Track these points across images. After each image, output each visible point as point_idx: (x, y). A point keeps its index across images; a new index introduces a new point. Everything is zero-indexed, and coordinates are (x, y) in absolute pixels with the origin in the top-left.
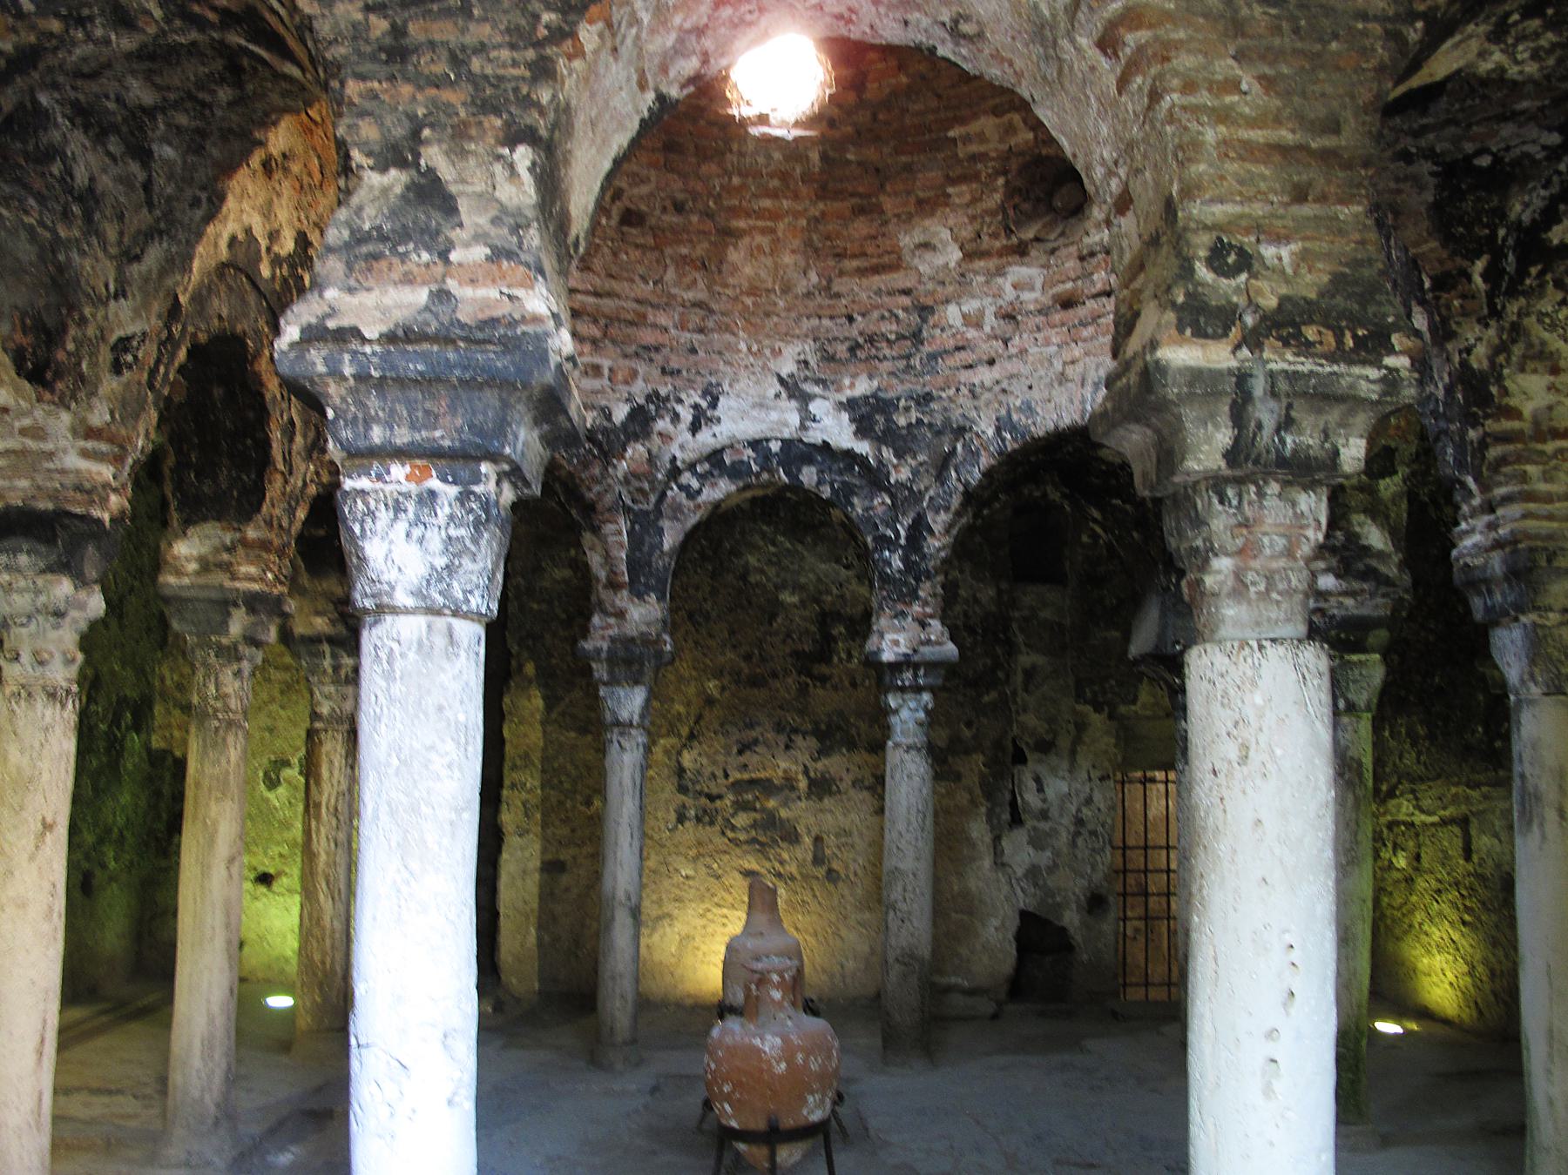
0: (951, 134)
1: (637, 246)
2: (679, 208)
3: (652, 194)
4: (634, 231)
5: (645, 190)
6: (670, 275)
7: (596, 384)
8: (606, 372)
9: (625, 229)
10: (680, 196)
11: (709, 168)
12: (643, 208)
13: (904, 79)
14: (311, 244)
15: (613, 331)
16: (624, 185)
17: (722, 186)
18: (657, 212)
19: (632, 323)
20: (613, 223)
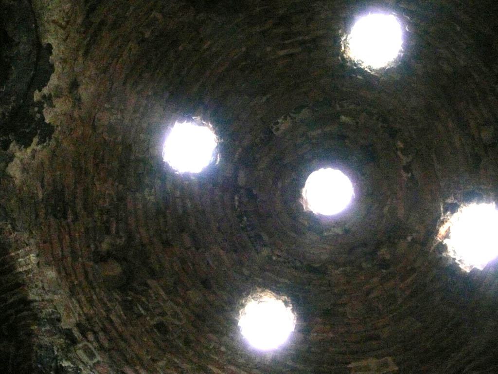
0: (350, 366)
1: (155, 342)
2: (187, 342)
3: (178, 326)
4: (159, 335)
5: (177, 323)
6: (161, 364)
7: (85, 358)
8: (95, 361)
9: (155, 330)
10: (192, 338)
11: (214, 337)
12: (170, 328)
13: (331, 335)
14: (50, 138)
15: (114, 353)
16: (169, 313)
17: (214, 348)
18: (175, 336)
19: (127, 361)
20: (153, 323)
